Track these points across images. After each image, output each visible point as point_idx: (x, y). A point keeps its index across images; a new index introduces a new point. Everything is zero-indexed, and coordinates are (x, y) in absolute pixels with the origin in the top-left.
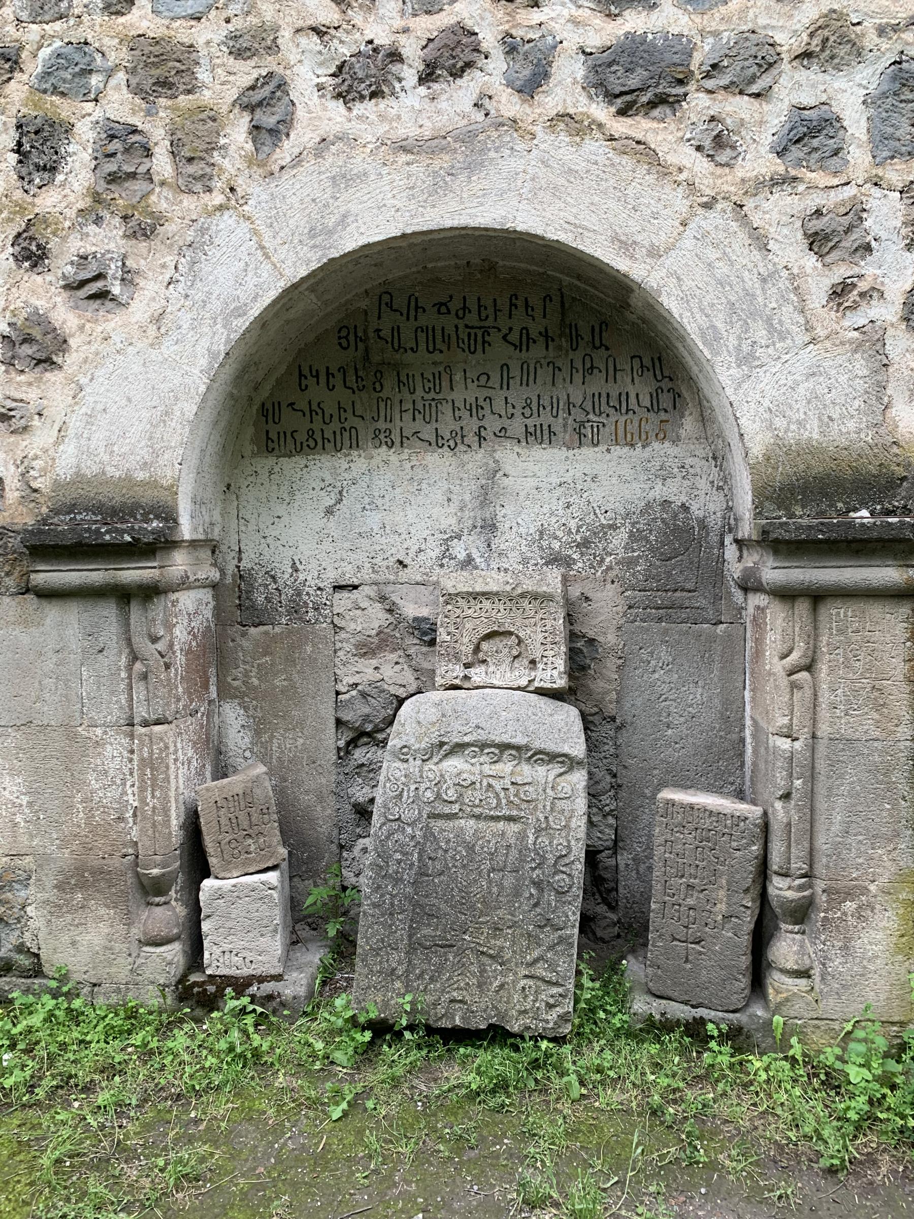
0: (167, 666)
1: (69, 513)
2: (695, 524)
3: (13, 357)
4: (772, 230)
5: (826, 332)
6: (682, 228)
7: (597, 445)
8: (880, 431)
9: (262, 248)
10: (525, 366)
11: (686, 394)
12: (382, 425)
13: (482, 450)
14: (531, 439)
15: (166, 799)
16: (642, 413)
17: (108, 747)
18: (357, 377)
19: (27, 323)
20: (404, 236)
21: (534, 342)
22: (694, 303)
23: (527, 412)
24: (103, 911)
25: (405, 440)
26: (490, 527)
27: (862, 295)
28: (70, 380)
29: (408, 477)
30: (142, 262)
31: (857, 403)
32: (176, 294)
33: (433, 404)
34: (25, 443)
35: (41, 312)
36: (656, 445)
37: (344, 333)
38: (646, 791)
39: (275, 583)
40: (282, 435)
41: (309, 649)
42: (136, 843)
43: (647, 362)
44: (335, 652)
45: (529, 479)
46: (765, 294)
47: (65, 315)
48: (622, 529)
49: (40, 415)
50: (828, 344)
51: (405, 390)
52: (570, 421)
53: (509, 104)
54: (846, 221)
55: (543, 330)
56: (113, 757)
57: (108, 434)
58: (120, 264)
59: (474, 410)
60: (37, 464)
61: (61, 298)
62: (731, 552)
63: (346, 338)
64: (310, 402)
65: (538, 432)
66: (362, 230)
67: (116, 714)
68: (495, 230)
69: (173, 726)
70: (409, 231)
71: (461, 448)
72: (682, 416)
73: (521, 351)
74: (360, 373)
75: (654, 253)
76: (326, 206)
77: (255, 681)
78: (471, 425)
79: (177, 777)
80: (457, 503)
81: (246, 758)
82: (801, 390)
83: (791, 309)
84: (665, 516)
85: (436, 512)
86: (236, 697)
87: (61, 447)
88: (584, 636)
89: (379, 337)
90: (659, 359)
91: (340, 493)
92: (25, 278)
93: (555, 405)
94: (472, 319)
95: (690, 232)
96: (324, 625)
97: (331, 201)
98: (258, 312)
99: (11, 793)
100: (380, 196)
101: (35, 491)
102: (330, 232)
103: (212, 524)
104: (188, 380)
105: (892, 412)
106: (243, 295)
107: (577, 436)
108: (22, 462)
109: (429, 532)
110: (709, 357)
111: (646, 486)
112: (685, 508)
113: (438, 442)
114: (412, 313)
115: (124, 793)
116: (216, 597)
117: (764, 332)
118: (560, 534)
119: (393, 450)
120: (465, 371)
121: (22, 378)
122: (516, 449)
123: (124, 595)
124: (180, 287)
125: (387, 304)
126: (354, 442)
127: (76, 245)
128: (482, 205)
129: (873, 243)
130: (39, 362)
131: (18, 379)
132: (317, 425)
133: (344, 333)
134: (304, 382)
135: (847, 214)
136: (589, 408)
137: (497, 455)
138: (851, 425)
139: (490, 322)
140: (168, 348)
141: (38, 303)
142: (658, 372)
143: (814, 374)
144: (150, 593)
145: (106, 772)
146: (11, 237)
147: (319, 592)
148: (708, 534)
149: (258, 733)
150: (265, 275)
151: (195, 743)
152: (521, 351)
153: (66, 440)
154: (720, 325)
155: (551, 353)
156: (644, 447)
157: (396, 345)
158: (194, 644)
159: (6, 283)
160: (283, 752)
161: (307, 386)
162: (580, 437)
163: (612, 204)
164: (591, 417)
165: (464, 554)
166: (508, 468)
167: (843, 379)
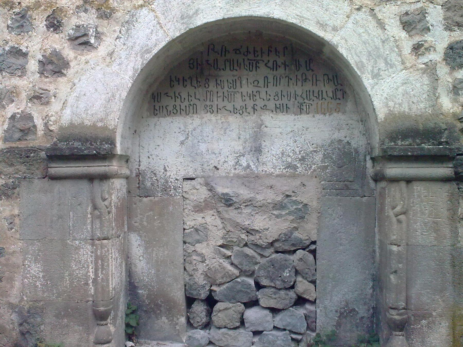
0: (109, 213)
1: (66, 141)
2: (353, 151)
3: (44, 70)
4: (386, 20)
5: (411, 65)
6: (347, 19)
7: (308, 114)
8: (435, 108)
9: (159, 23)
10: (275, 78)
11: (348, 92)
12: (208, 103)
13: (255, 115)
14: (278, 110)
15: (107, 275)
16: (329, 99)
17: (82, 250)
18: (197, 81)
19: (51, 55)
20: (224, 19)
21: (279, 67)
22: (353, 51)
23: (276, 98)
24: (76, 328)
25: (219, 110)
26: (258, 150)
27: (426, 49)
28: (69, 81)
29: (220, 127)
30: (105, 29)
31: (425, 96)
32: (120, 43)
33: (232, 94)
34: (47, 109)
35: (57, 50)
36: (335, 114)
37: (191, 62)
38: (330, 275)
39: (156, 176)
40: (161, 107)
41: (171, 208)
42: (93, 295)
43: (331, 77)
44: (184, 209)
45: (277, 129)
46: (384, 47)
47: (69, 53)
48: (320, 153)
49: (55, 97)
50: (411, 70)
51: (219, 87)
52: (296, 102)
54: (418, 17)
55: (284, 62)
56: (84, 254)
57: (86, 105)
58: (95, 29)
59: (252, 97)
60: (53, 119)
61: (67, 45)
62: (369, 164)
63: (192, 64)
64: (175, 93)
65: (281, 107)
66: (205, 17)
67: (86, 234)
68: (265, 18)
69: (111, 241)
70: (226, 17)
71: (245, 114)
72: (347, 102)
73: (273, 71)
74: (199, 80)
75: (335, 29)
76: (189, 6)
77: (145, 223)
78: (250, 103)
79: (112, 265)
80: (243, 140)
81: (140, 260)
82: (400, 90)
83: (395, 54)
84: (339, 147)
85: (233, 143)
86: (136, 231)
87: (64, 111)
88: (302, 203)
89: (208, 64)
90: (336, 76)
91: (188, 134)
92: (51, 35)
93: (289, 95)
94: (251, 56)
95: (351, 21)
96: (179, 197)
97: (191, 4)
98: (157, 51)
99: (35, 271)
100: (213, 2)
101: (51, 131)
102: (190, 17)
103: (128, 148)
104: (123, 81)
105: (440, 100)
106: (150, 44)
107: (299, 110)
108: (46, 118)
109: (229, 153)
110: (360, 75)
111: (331, 133)
112: (349, 143)
113: (235, 111)
114: (223, 53)
115: (89, 272)
116: (128, 183)
117: (384, 64)
118: (291, 154)
119: (213, 115)
120: (247, 79)
121: (47, 80)
122: (271, 115)
123: (91, 178)
124: (122, 40)
125: (212, 49)
126: (195, 110)
127: (74, 21)
128: (259, 7)
129: (431, 27)
130: (56, 72)
131: (46, 80)
132: (178, 101)
133: (191, 62)
134: (172, 83)
135: (419, 14)
136: (305, 97)
137: (263, 118)
138: (422, 105)
139: (259, 58)
140: (115, 67)
141: (56, 46)
142: (336, 82)
143: (406, 83)
144: (104, 177)
145: (80, 261)
146: (45, 17)
147: (176, 181)
148: (359, 155)
149: (146, 248)
150: (160, 35)
151: (119, 251)
152: (273, 71)
153: (66, 108)
154: (364, 61)
155: (287, 72)
156: (330, 115)
157: (216, 67)
158: (119, 204)
159: (42, 37)
160: (157, 258)
161: (173, 85)
162: (301, 110)
163: (316, 8)
164: (306, 101)
165: (246, 164)
166: (267, 124)
167: (418, 85)
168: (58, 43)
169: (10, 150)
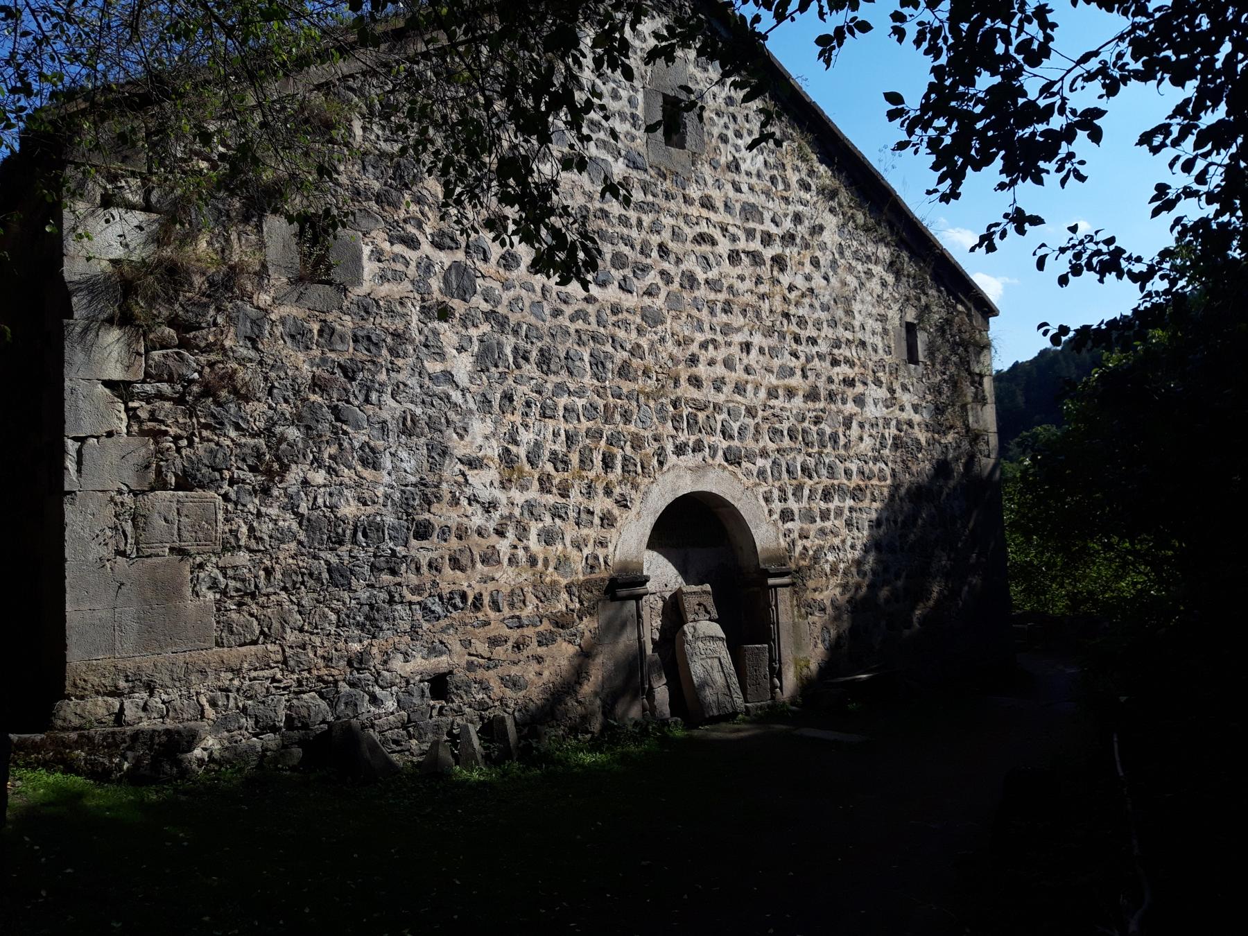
47: (616, 511)
53: (709, 460)
168: (609, 504)
169: (587, 581)
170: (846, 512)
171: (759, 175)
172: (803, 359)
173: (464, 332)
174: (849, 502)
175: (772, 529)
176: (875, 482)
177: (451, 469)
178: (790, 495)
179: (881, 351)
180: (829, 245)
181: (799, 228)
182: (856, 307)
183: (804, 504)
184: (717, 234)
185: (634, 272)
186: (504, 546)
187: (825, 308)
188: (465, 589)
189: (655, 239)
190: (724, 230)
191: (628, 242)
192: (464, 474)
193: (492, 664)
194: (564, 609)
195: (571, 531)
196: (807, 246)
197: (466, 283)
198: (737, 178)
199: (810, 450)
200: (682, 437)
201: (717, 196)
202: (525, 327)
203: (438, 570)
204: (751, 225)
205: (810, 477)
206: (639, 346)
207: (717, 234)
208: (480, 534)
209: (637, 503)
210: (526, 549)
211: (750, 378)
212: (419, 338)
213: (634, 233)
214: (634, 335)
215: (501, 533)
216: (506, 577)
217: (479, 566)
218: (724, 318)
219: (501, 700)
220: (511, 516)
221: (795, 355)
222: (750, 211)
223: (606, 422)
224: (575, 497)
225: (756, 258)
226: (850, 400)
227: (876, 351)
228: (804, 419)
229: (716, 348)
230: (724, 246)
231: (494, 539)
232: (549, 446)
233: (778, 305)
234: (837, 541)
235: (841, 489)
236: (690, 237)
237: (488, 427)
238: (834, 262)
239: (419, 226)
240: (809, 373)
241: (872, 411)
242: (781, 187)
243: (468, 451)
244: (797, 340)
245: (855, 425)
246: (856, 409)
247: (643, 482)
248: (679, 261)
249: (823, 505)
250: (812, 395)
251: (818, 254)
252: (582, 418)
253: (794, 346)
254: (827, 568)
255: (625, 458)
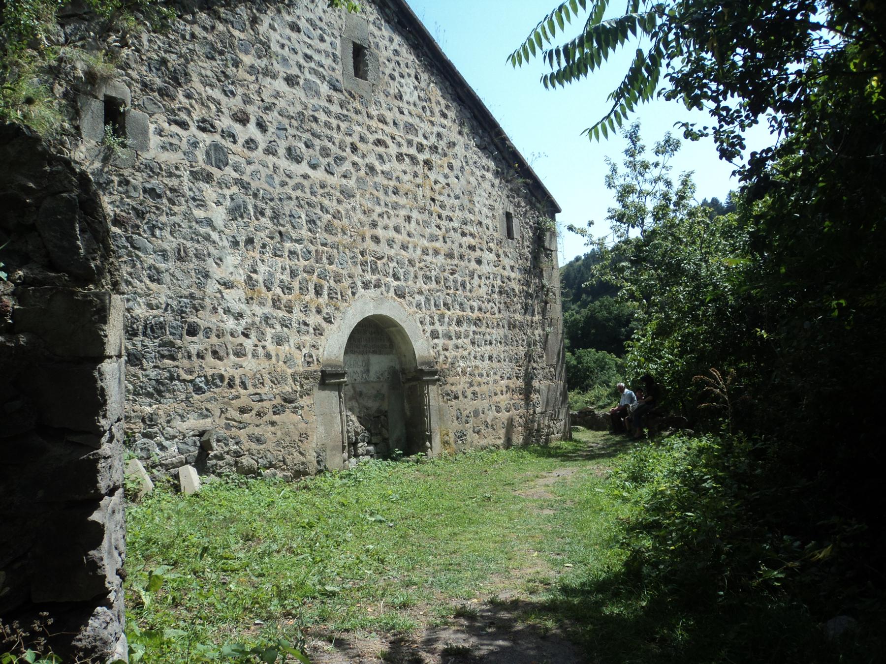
53: (385, 293)
168: (319, 319)
170: (471, 334)
171: (415, 105)
172: (443, 230)
173: (220, 191)
174: (473, 328)
175: (425, 343)
176: (488, 315)
177: (212, 287)
178: (436, 321)
179: (491, 229)
180: (459, 156)
181: (441, 142)
182: (476, 199)
183: (445, 327)
184: (389, 141)
185: (335, 161)
186: (248, 344)
187: (457, 197)
188: (223, 373)
189: (349, 140)
190: (393, 138)
191: (330, 139)
192: (220, 292)
193: (241, 426)
194: (290, 390)
195: (294, 339)
196: (445, 155)
197: (222, 157)
198: (401, 105)
199: (448, 291)
200: (368, 276)
201: (389, 116)
202: (262, 192)
203: (202, 358)
204: (410, 137)
205: (449, 309)
206: (339, 212)
207: (389, 141)
208: (232, 335)
209: (338, 320)
210: (264, 347)
211: (411, 240)
212: (189, 194)
213: (334, 134)
214: (335, 203)
215: (246, 336)
216: (249, 364)
217: (232, 357)
218: (394, 198)
219: (248, 450)
220: (253, 323)
221: (438, 227)
222: (410, 128)
223: (317, 262)
224: (297, 315)
225: (413, 159)
226: (473, 260)
227: (488, 228)
228: (445, 270)
229: (389, 217)
230: (393, 150)
231: (241, 339)
232: (278, 275)
233: (429, 194)
234: (466, 353)
235: (469, 320)
236: (371, 141)
237: (237, 260)
238: (462, 167)
239: (189, 113)
240: (447, 240)
241: (485, 269)
242: (429, 114)
243: (223, 276)
244: (440, 217)
245: (476, 277)
246: (477, 266)
247: (342, 305)
248: (364, 156)
249: (457, 329)
250: (450, 256)
251: (452, 161)
252: (301, 259)
253: (439, 220)
254: (459, 370)
255: (330, 289)
